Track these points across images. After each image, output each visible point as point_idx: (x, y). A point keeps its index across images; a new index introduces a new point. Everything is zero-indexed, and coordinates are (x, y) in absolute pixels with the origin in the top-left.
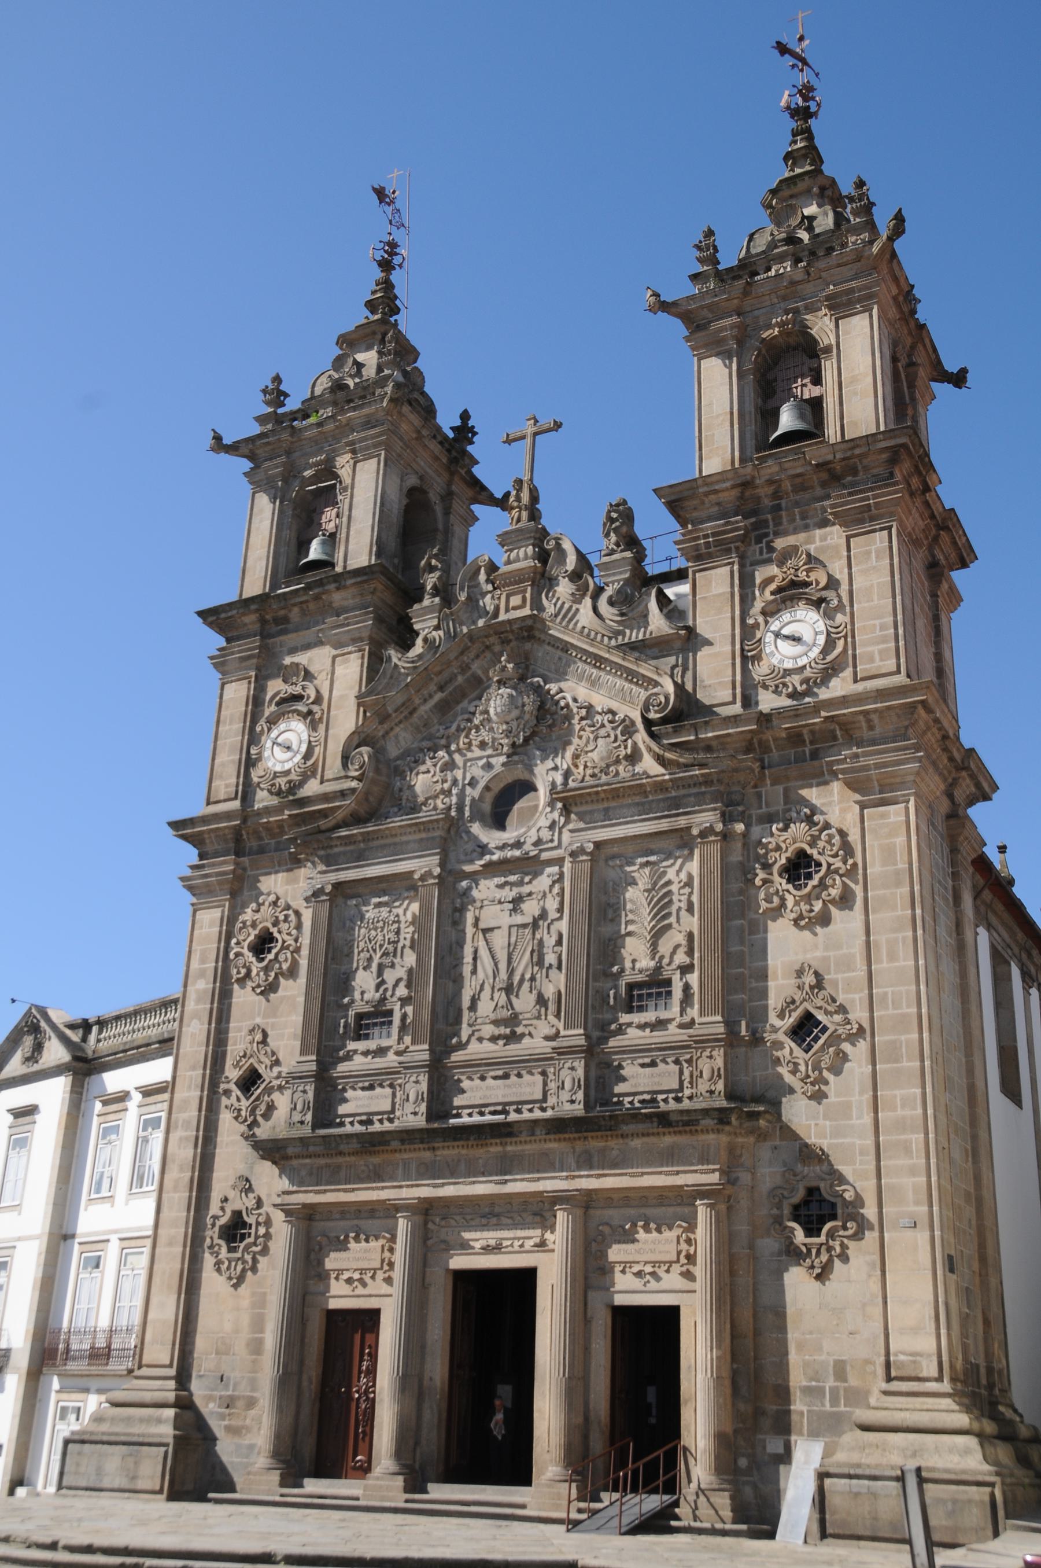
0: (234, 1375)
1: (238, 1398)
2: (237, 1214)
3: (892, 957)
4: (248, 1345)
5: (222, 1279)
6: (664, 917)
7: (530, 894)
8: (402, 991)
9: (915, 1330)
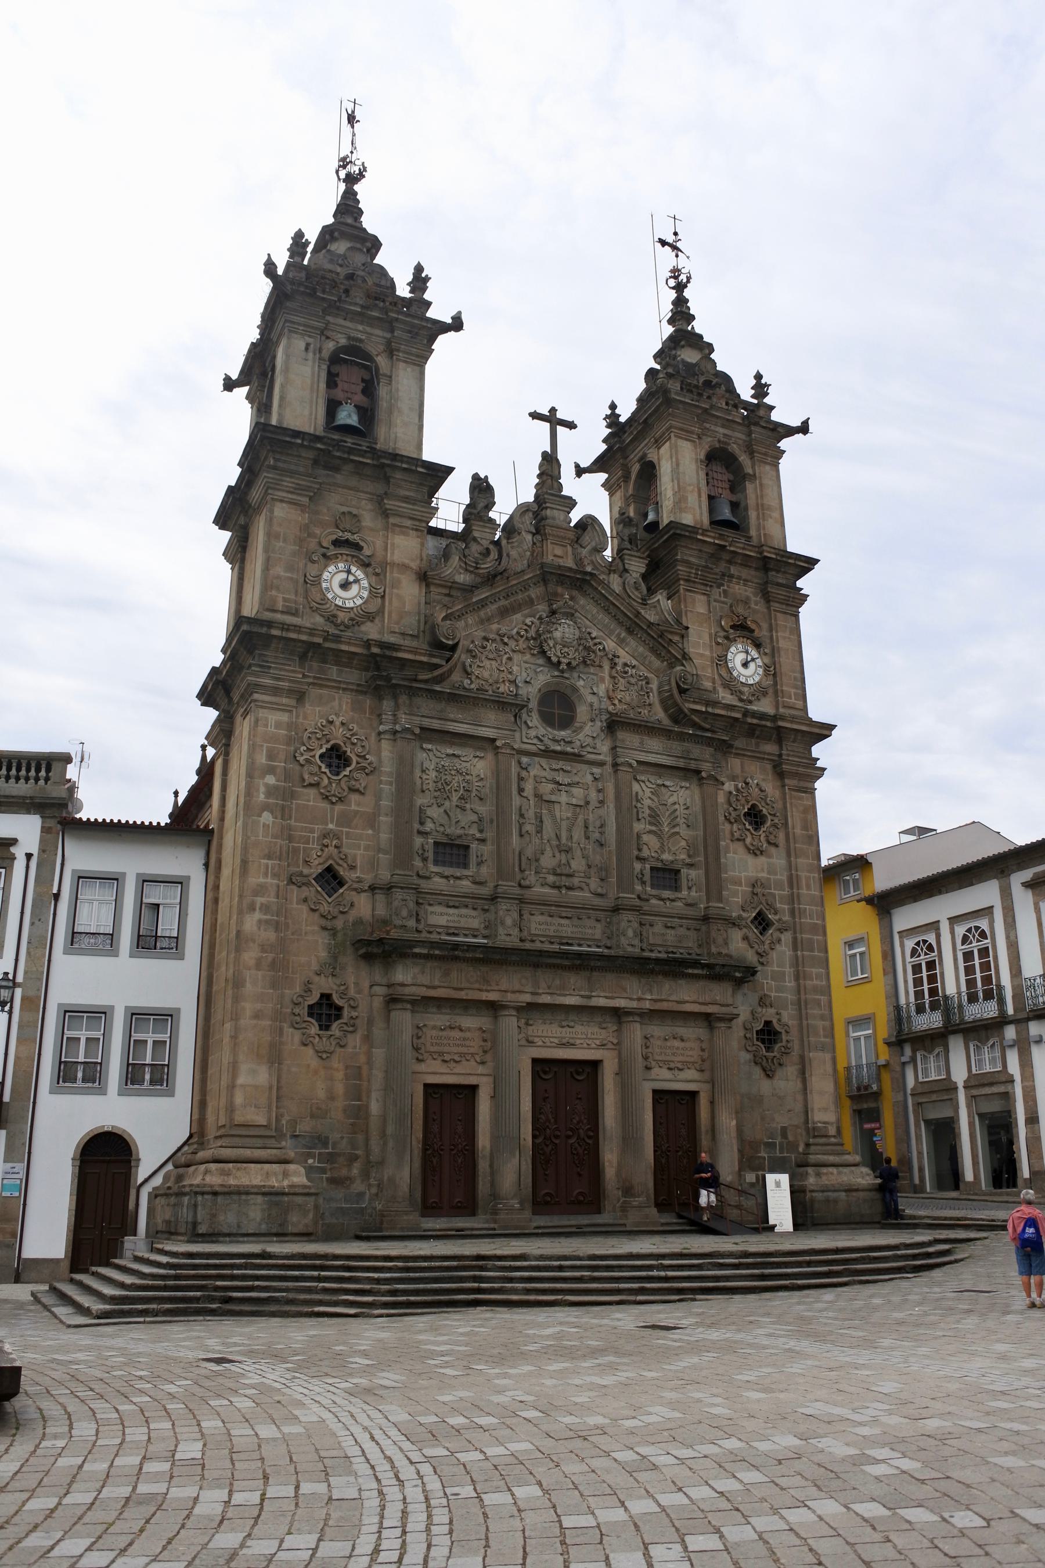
0: (334, 1136)
1: (339, 1155)
2: (326, 997)
3: (808, 888)
4: (345, 1111)
5: (309, 1051)
6: (674, 826)
7: (578, 783)
8: (474, 831)
9: (825, 1109)
